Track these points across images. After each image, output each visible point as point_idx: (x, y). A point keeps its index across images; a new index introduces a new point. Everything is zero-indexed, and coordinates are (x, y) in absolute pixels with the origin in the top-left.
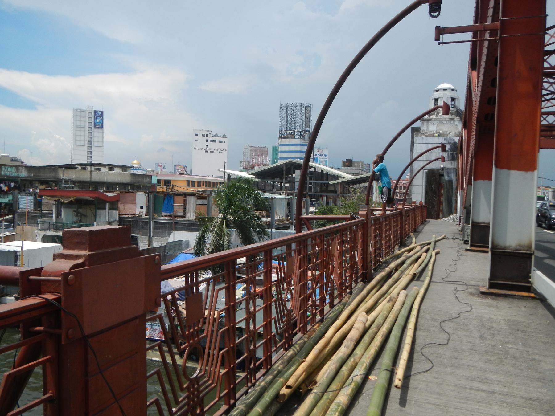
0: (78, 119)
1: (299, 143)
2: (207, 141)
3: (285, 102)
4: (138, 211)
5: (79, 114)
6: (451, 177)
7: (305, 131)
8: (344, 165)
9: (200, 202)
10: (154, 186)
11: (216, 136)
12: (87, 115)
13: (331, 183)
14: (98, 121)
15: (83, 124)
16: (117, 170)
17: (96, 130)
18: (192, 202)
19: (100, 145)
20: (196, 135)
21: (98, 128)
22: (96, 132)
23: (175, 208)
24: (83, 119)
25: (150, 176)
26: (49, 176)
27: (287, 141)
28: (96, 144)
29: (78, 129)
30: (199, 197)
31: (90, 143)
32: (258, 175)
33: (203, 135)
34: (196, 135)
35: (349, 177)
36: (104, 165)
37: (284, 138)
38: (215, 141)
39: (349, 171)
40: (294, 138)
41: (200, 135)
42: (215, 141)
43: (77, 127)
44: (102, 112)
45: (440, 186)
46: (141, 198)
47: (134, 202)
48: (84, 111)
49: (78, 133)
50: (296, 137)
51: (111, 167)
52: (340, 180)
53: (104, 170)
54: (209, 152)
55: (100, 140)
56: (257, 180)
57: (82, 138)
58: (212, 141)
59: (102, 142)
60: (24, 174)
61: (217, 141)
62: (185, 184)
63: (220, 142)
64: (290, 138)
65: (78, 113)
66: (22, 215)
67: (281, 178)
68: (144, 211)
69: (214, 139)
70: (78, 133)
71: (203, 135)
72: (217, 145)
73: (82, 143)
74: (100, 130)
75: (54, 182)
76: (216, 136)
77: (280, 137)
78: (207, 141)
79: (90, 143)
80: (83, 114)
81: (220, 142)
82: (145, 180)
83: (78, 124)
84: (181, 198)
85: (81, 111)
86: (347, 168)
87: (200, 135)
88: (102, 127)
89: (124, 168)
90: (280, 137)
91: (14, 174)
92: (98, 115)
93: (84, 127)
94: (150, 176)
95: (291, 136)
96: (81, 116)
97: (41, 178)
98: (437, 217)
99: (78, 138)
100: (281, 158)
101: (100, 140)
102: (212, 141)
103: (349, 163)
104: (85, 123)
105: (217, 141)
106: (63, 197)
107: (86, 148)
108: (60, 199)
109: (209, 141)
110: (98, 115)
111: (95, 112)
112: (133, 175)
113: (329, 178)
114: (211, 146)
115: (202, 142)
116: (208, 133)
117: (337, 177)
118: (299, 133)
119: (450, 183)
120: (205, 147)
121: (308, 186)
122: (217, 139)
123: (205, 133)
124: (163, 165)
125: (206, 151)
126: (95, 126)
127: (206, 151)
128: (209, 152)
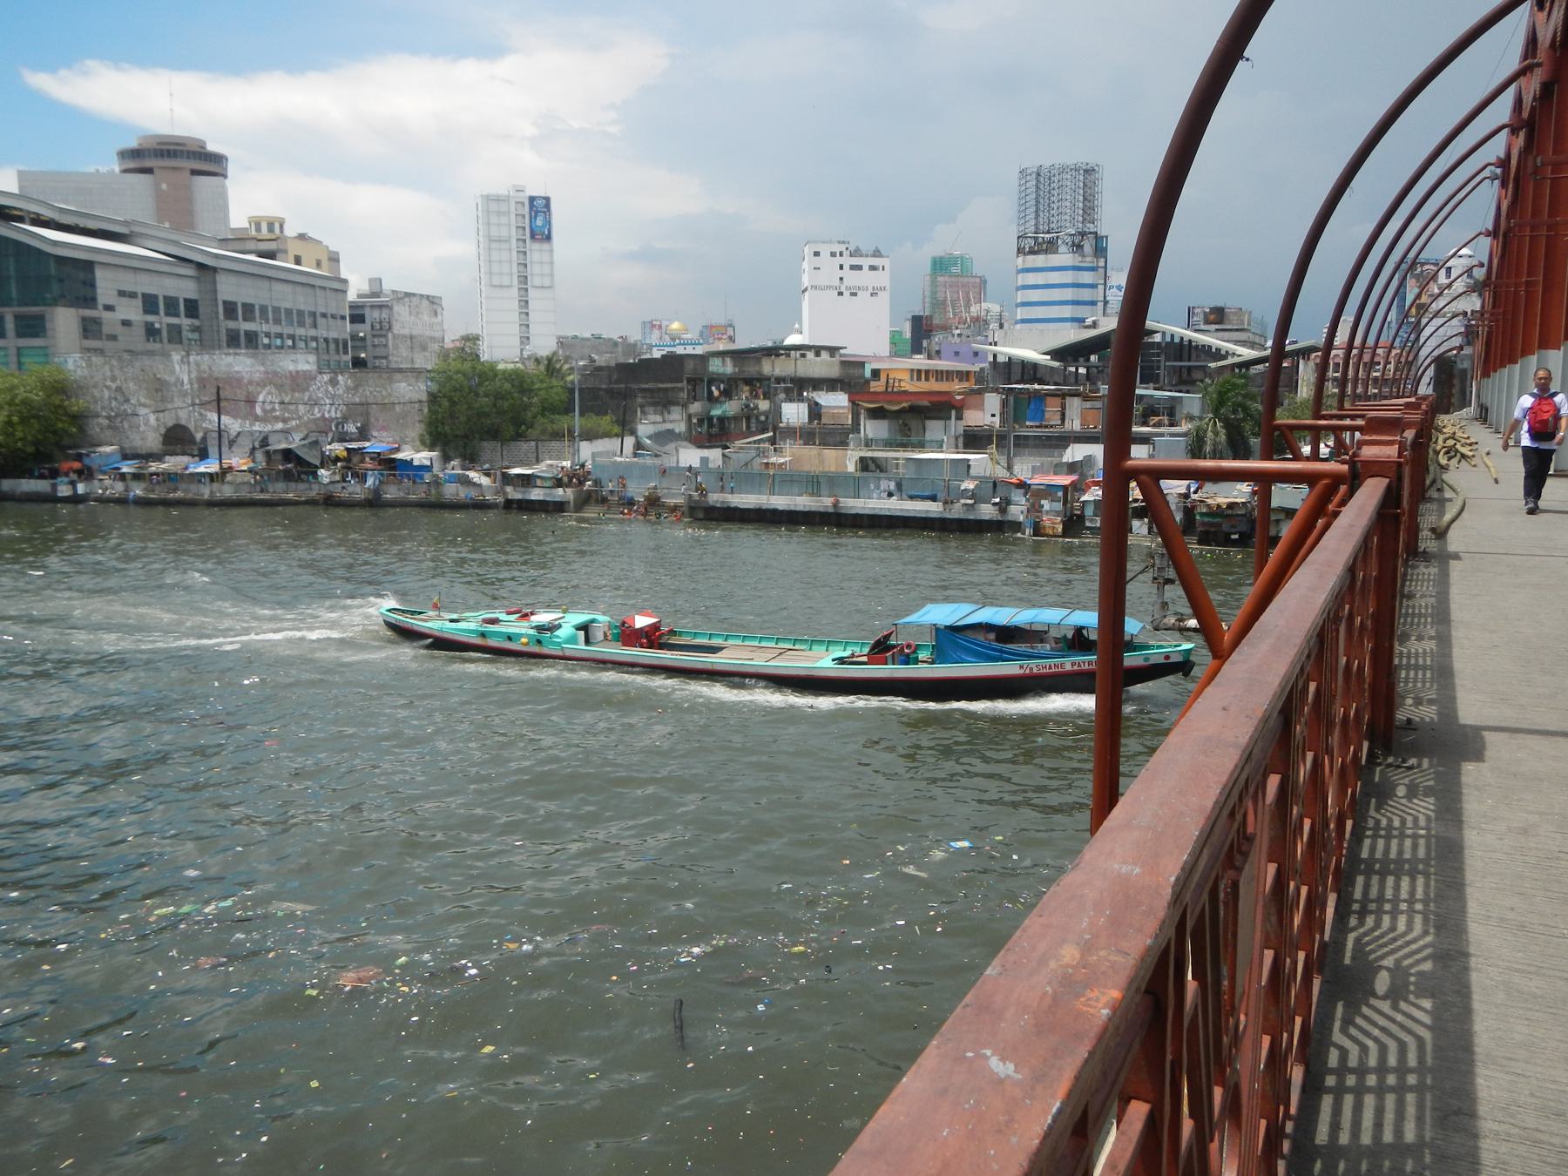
0: (494, 219)
1: (1070, 263)
2: (841, 267)
3: (1032, 163)
4: (988, 420)
5: (493, 207)
6: (1466, 365)
7: (1083, 234)
8: (1207, 322)
9: (1089, 404)
10: (867, 382)
11: (856, 253)
12: (513, 209)
13: (1212, 365)
14: (539, 222)
15: (504, 233)
16: (825, 355)
17: (536, 246)
18: (1074, 405)
19: (547, 283)
20: (817, 254)
21: (541, 240)
22: (536, 251)
23: (1047, 415)
24: (504, 220)
25: (862, 364)
26: (751, 370)
27: (1039, 260)
28: (537, 281)
29: (494, 245)
30: (1086, 398)
31: (524, 279)
32: (1057, 354)
33: (833, 254)
34: (817, 254)
35: (1247, 353)
36: (808, 348)
37: (1032, 252)
38: (859, 268)
39: (1227, 335)
40: (1056, 252)
41: (825, 253)
42: (859, 268)
43: (491, 240)
44: (547, 199)
45: (1451, 376)
46: (993, 402)
47: (981, 407)
48: (506, 199)
49: (495, 256)
50: (1063, 248)
51: (818, 350)
52: (1230, 361)
53: (810, 355)
54: (847, 294)
55: (546, 270)
56: (1056, 364)
57: (506, 268)
58: (853, 267)
59: (552, 275)
60: (728, 368)
61: (866, 268)
62: (906, 377)
63: (873, 268)
64: (1046, 252)
65: (492, 202)
66: (791, 432)
67: (1076, 360)
68: (997, 420)
69: (856, 261)
70: (495, 256)
71: (833, 254)
72: (865, 278)
73: (506, 281)
74: (545, 246)
75: (759, 380)
76: (856, 253)
77: (1020, 251)
78: (841, 267)
79: (524, 279)
80: (503, 207)
81: (873, 268)
82: (856, 372)
83: (494, 232)
84: (1058, 400)
85: (498, 199)
86: (1214, 327)
87: (825, 253)
88: (548, 238)
89: (833, 350)
90: (1020, 251)
91: (721, 370)
92: (539, 207)
93: (508, 241)
94: (862, 364)
95: (1050, 247)
96: (499, 213)
97: (745, 375)
98: (1447, 412)
99: (496, 268)
100: (1024, 304)
101: (546, 270)
102: (853, 267)
103: (1217, 316)
104: (509, 227)
105: (866, 268)
106: (890, 402)
107: (515, 292)
108: (886, 406)
109: (846, 267)
110: (539, 207)
111: (532, 199)
112: (843, 363)
113: (1194, 356)
114: (852, 279)
115: (829, 271)
116: (842, 248)
117: (1218, 355)
118: (1069, 240)
119: (1464, 371)
120: (837, 282)
121: (1161, 372)
122: (865, 262)
123: (837, 248)
124: (664, 323)
125: (841, 294)
126: (533, 236)
127: (841, 294)
128: (847, 294)
